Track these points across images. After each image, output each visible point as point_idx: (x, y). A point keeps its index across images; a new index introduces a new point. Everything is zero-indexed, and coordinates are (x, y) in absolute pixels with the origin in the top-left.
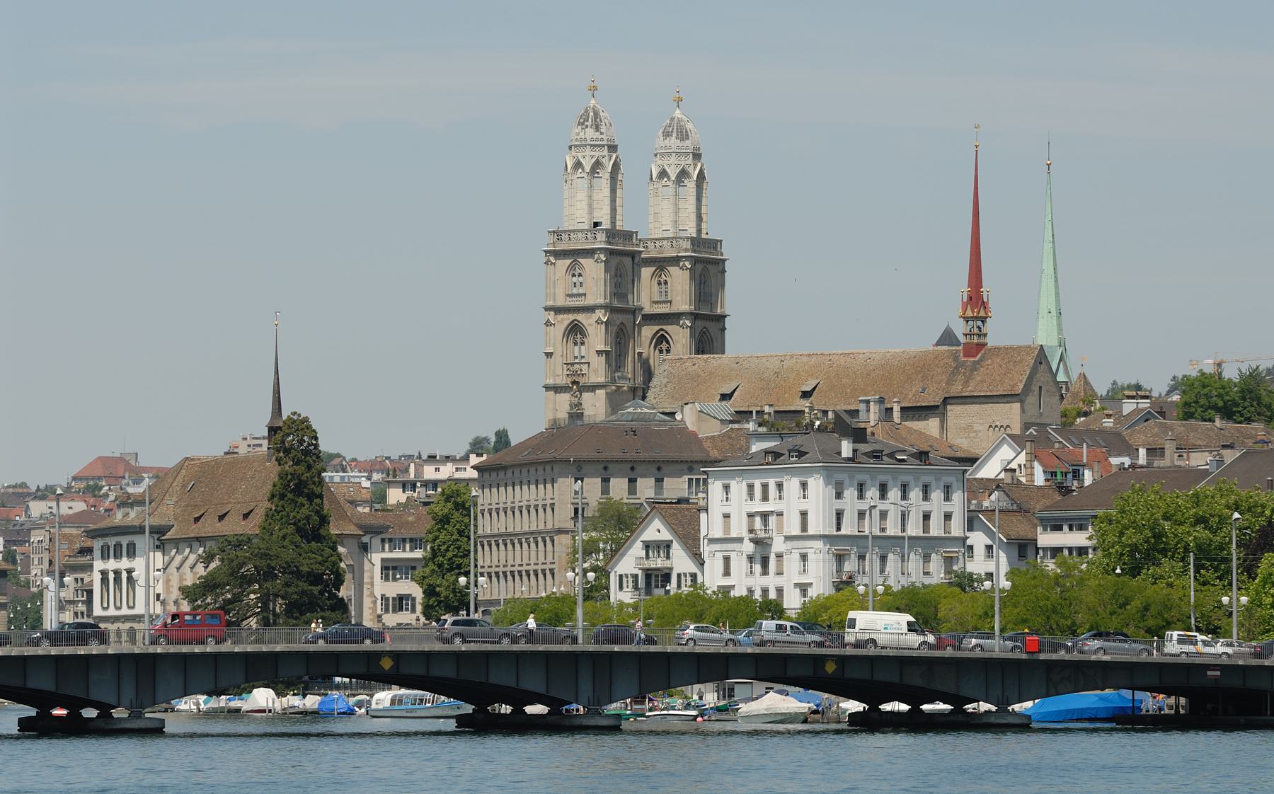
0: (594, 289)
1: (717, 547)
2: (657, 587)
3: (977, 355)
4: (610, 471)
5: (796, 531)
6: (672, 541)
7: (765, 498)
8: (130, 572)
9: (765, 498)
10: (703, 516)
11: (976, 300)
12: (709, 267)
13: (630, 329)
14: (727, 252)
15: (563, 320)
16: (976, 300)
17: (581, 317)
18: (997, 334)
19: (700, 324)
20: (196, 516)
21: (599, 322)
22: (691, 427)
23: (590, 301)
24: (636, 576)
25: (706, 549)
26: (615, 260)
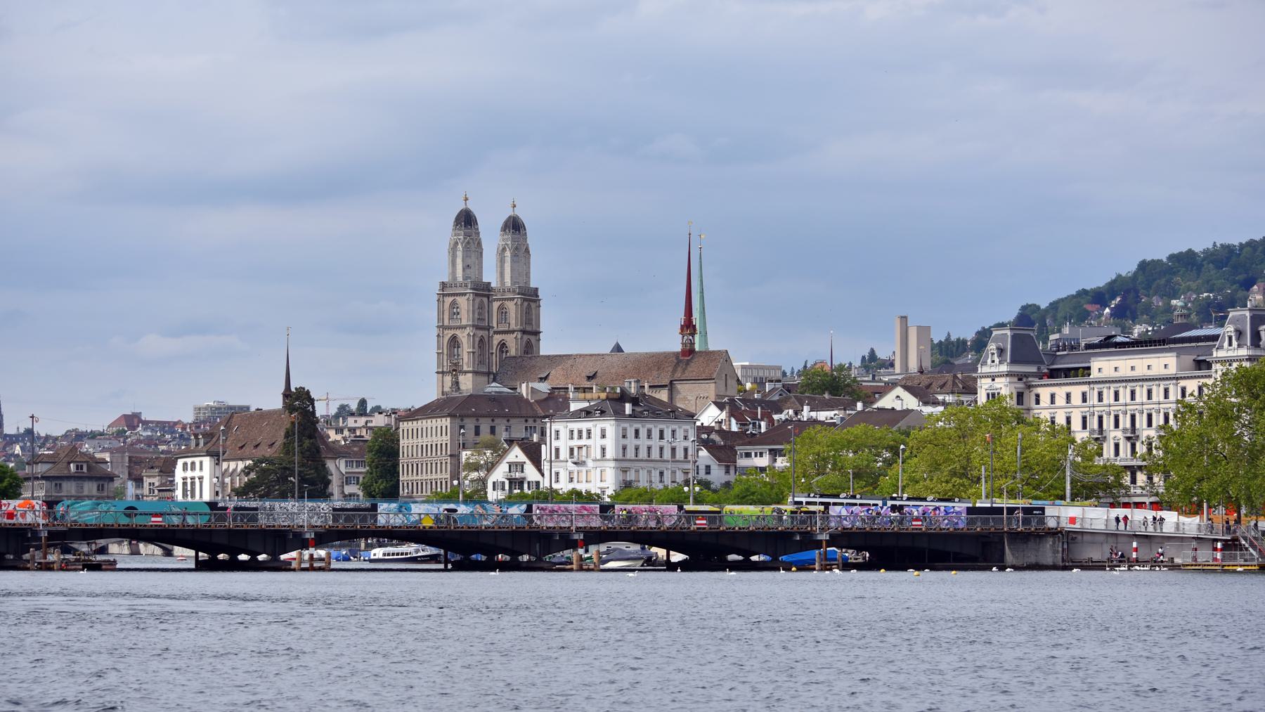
0: (466, 316)
2: (515, 489)
3: (689, 355)
4: (480, 422)
5: (599, 457)
6: (525, 462)
7: (580, 437)
9: (580, 437)
12: (531, 303)
13: (486, 340)
14: (539, 294)
15: (448, 334)
16: (688, 326)
17: (458, 332)
19: (526, 337)
20: (240, 445)
21: (469, 335)
23: (464, 322)
24: (503, 483)
25: (546, 467)
26: (478, 300)
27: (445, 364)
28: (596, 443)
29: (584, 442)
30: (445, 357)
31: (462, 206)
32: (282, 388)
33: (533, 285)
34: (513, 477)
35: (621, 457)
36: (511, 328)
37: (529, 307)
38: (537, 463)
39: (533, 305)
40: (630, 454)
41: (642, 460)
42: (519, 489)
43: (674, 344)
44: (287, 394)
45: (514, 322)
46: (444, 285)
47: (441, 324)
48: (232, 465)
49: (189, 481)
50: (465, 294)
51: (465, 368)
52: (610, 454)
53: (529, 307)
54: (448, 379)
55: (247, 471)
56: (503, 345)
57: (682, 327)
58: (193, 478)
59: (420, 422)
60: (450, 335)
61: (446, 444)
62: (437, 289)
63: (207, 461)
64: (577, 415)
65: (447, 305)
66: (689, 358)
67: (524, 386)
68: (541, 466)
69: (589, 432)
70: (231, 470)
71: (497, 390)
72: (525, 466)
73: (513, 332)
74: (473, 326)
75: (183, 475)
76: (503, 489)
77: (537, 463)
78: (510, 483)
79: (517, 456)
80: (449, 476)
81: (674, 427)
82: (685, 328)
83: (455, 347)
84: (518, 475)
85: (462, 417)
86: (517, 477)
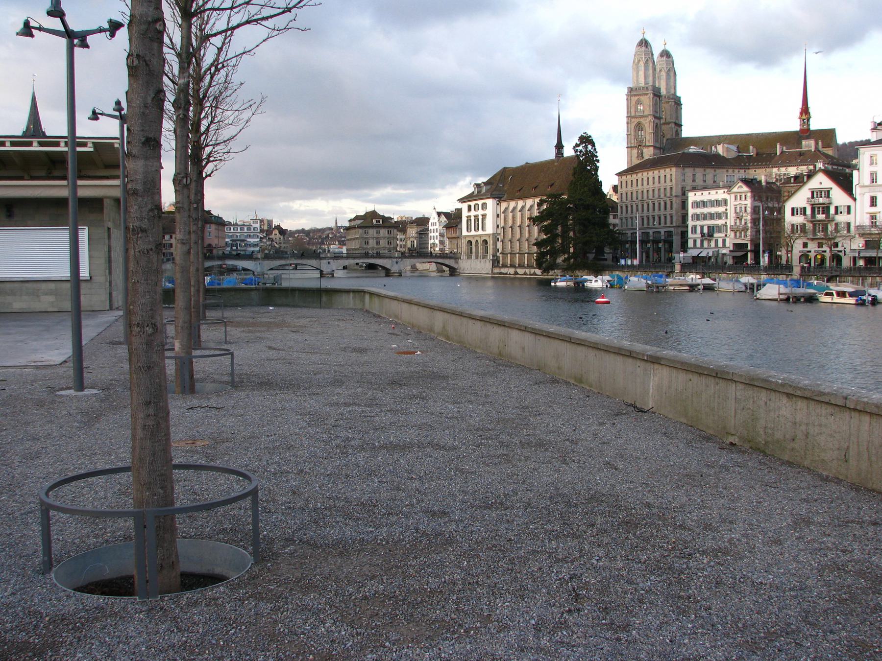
0: (648, 109)
1: (866, 190)
2: (819, 214)
6: (831, 188)
10: (855, 173)
11: (805, 111)
15: (634, 121)
16: (805, 111)
17: (642, 120)
21: (650, 121)
23: (646, 113)
24: (805, 208)
25: (857, 191)
26: (655, 98)
31: (641, 38)
32: (555, 142)
34: (817, 202)
36: (667, 121)
37: (677, 108)
38: (846, 185)
39: (679, 108)
42: (823, 214)
43: (794, 125)
44: (559, 146)
45: (669, 117)
46: (631, 90)
48: (512, 204)
49: (473, 218)
51: (648, 144)
53: (677, 108)
54: (635, 151)
57: (801, 114)
58: (476, 216)
59: (640, 175)
61: (671, 188)
63: (490, 202)
65: (633, 103)
68: (852, 192)
70: (511, 208)
71: (695, 150)
73: (669, 123)
74: (653, 116)
75: (468, 214)
76: (805, 214)
77: (846, 185)
78: (813, 210)
79: (821, 183)
80: (674, 212)
82: (804, 114)
83: (639, 130)
84: (821, 200)
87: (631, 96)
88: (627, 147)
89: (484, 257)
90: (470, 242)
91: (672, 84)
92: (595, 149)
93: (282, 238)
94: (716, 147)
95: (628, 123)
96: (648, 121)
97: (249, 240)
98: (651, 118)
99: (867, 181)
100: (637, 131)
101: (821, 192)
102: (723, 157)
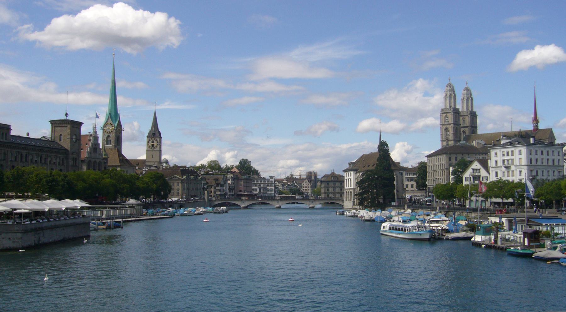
1: (494, 169)
2: (476, 180)
3: (537, 130)
6: (480, 168)
7: (508, 155)
8: (351, 179)
10: (489, 161)
11: (536, 120)
14: (477, 114)
15: (444, 127)
16: (536, 120)
17: (448, 126)
18: (541, 126)
21: (452, 127)
22: (475, 145)
23: (450, 123)
25: (490, 170)
26: (455, 114)
27: (443, 138)
28: (516, 156)
29: (510, 157)
30: (443, 135)
33: (474, 110)
34: (475, 175)
35: (529, 164)
36: (467, 126)
38: (486, 167)
40: (534, 163)
41: (539, 166)
46: (442, 110)
47: (442, 124)
50: (450, 112)
51: (451, 139)
52: (524, 161)
55: (362, 175)
56: (464, 132)
57: (533, 121)
60: (445, 128)
62: (440, 111)
64: (505, 145)
66: (536, 132)
67: (474, 142)
68: (488, 170)
69: (512, 152)
72: (480, 170)
77: (486, 167)
79: (476, 165)
80: (445, 177)
81: (554, 149)
83: (447, 132)
84: (477, 174)
85: (450, 154)
86: (477, 175)
87: (442, 113)
88: (441, 141)
89: (351, 200)
90: (347, 192)
91: (470, 105)
92: (388, 148)
93: (310, 184)
94: (473, 142)
95: (441, 128)
96: (450, 127)
97: (268, 187)
98: (452, 125)
99: (494, 165)
100: (446, 132)
101: (476, 170)
102: (476, 147)
